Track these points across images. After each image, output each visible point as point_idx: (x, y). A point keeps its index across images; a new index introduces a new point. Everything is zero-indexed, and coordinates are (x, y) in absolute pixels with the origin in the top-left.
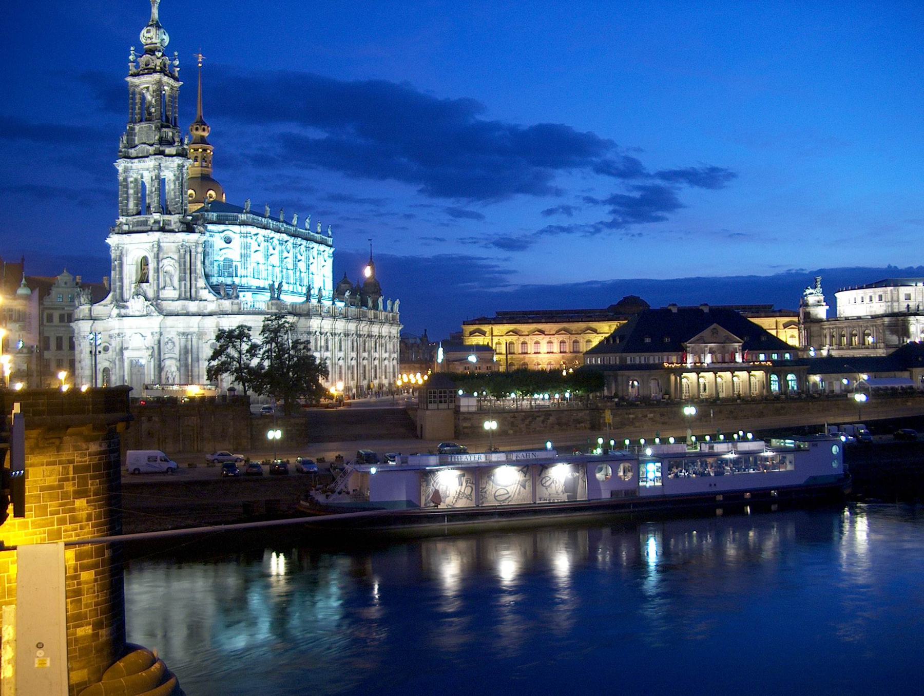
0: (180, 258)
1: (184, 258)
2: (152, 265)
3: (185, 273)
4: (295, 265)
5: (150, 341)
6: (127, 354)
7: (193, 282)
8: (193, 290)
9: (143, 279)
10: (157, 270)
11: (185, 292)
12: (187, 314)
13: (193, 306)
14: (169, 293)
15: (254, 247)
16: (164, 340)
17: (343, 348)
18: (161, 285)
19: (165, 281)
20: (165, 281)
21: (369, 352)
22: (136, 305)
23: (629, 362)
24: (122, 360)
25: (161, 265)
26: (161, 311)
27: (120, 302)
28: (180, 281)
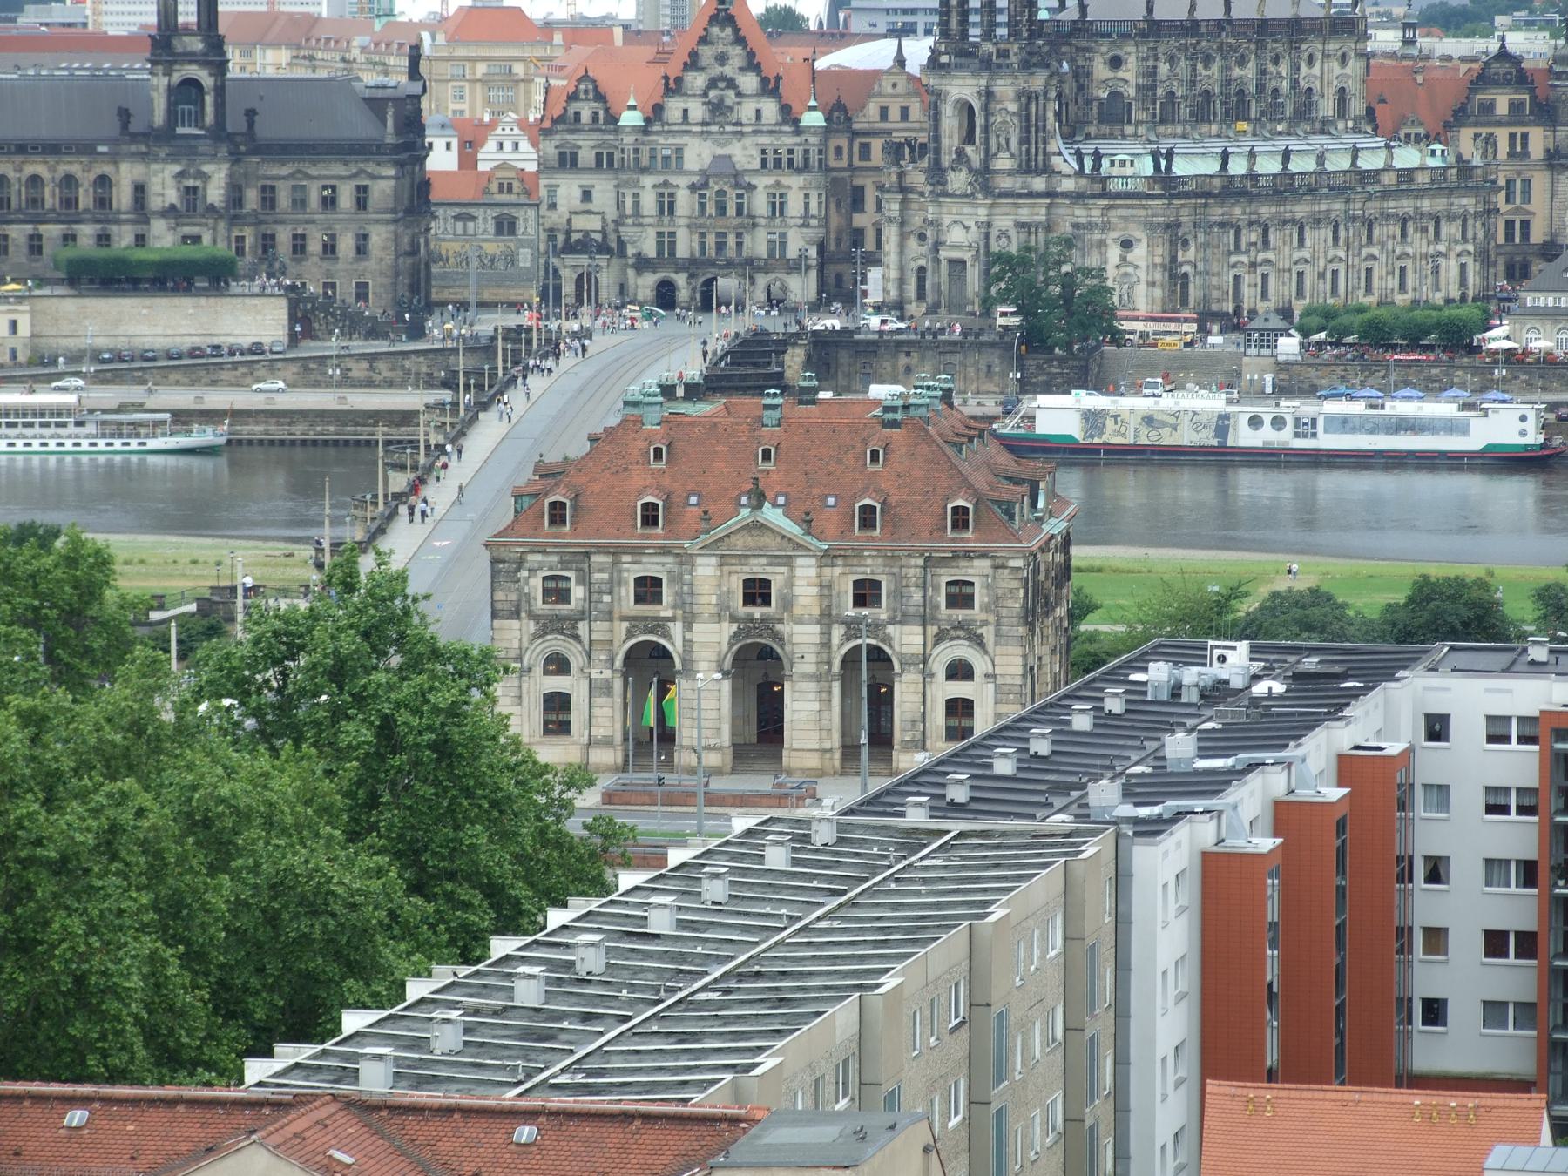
0: (1020, 109)
1: (1027, 108)
2: (979, 121)
3: (1028, 132)
4: (1261, 87)
5: (974, 235)
6: (943, 254)
7: (1041, 146)
8: (1040, 158)
9: (969, 138)
10: (986, 129)
11: (1028, 160)
12: (1030, 195)
13: (1039, 184)
14: (1003, 163)
15: (1164, 68)
16: (994, 233)
17: (1308, 242)
18: (994, 149)
19: (999, 144)
20: (999, 144)
21: (1383, 245)
22: (958, 180)
23: (1529, 304)
24: (937, 261)
25: (992, 119)
26: (988, 191)
27: (937, 174)
28: (1021, 143)
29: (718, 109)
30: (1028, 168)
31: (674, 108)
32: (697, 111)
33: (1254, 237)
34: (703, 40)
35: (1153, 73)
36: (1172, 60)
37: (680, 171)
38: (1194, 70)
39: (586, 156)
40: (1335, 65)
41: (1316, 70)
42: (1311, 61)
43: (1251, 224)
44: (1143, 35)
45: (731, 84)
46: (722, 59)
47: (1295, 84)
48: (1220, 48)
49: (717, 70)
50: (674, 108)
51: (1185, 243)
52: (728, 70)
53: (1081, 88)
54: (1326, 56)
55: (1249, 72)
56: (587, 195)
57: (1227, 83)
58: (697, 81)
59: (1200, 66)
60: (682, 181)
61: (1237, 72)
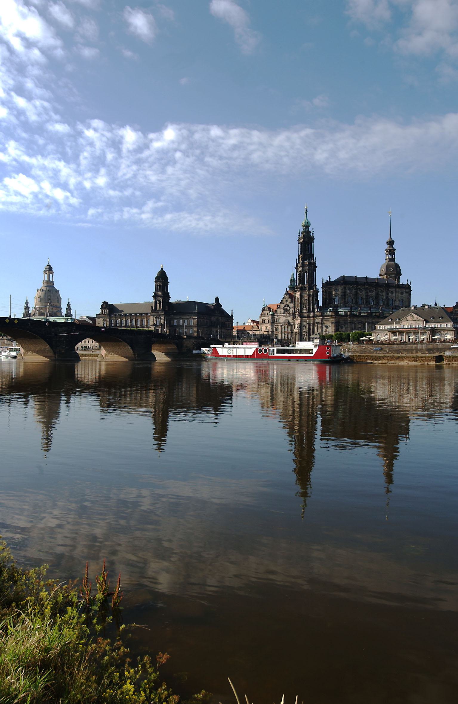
14: (305, 310)
29: (286, 310)
30: (309, 312)
31: (278, 311)
32: (282, 311)
33: (360, 326)
34: (283, 298)
35: (345, 292)
36: (350, 289)
37: (279, 323)
38: (357, 292)
39: (266, 321)
40: (400, 295)
41: (394, 295)
42: (392, 293)
43: (359, 323)
44: (342, 284)
45: (288, 306)
46: (286, 301)
47: (387, 297)
48: (364, 288)
49: (286, 303)
50: (278, 311)
51: (342, 327)
52: (288, 303)
53: (329, 296)
54: (396, 292)
55: (374, 294)
56: (266, 328)
57: (367, 296)
58: (282, 305)
59: (359, 292)
60: (280, 324)
61: (370, 294)
